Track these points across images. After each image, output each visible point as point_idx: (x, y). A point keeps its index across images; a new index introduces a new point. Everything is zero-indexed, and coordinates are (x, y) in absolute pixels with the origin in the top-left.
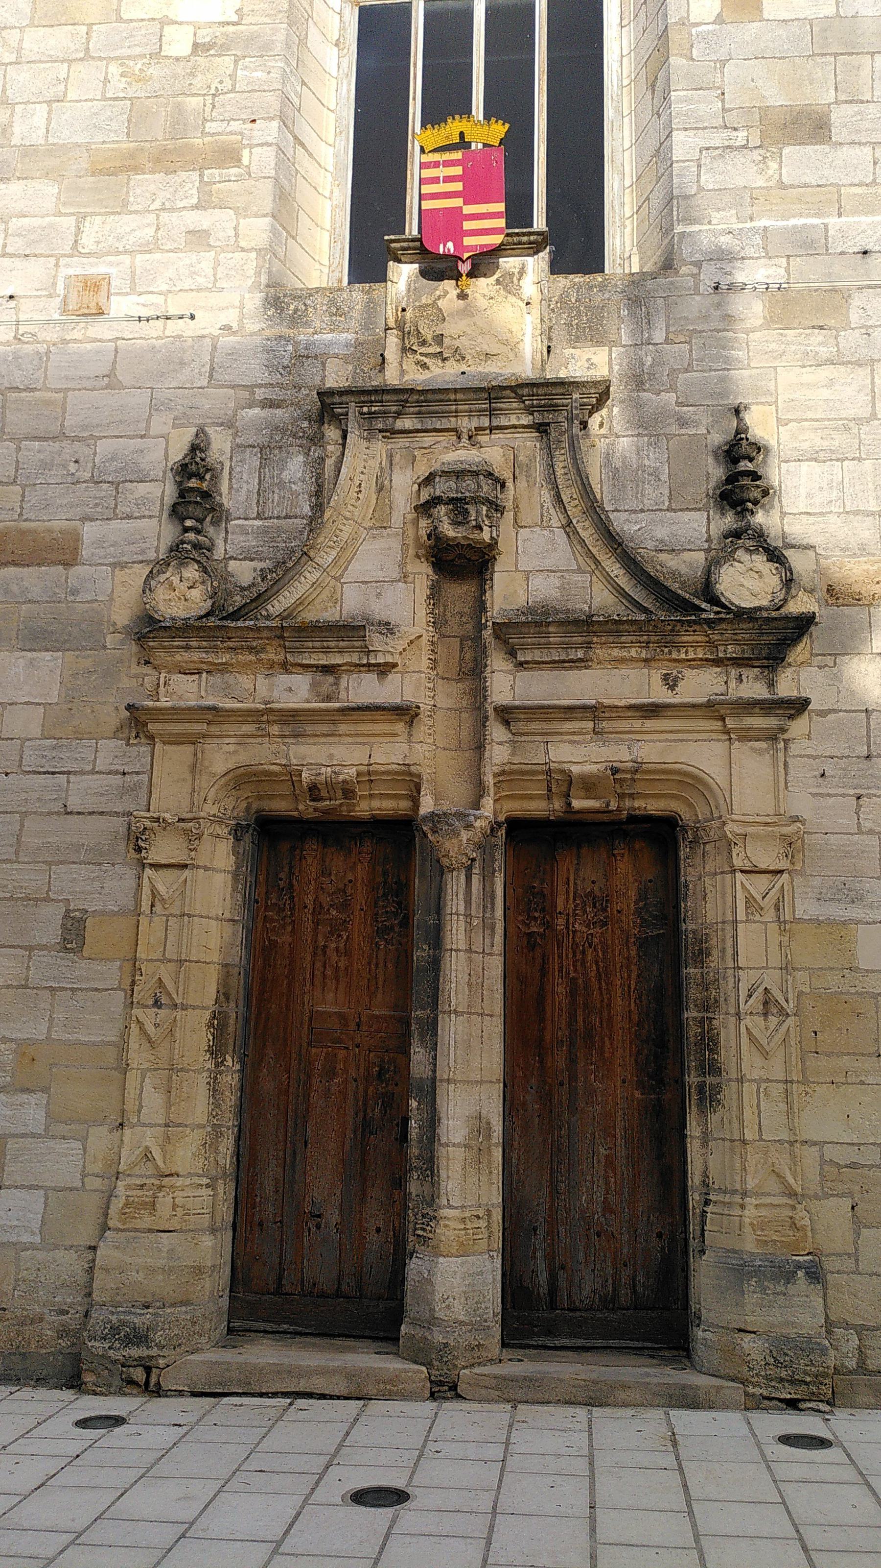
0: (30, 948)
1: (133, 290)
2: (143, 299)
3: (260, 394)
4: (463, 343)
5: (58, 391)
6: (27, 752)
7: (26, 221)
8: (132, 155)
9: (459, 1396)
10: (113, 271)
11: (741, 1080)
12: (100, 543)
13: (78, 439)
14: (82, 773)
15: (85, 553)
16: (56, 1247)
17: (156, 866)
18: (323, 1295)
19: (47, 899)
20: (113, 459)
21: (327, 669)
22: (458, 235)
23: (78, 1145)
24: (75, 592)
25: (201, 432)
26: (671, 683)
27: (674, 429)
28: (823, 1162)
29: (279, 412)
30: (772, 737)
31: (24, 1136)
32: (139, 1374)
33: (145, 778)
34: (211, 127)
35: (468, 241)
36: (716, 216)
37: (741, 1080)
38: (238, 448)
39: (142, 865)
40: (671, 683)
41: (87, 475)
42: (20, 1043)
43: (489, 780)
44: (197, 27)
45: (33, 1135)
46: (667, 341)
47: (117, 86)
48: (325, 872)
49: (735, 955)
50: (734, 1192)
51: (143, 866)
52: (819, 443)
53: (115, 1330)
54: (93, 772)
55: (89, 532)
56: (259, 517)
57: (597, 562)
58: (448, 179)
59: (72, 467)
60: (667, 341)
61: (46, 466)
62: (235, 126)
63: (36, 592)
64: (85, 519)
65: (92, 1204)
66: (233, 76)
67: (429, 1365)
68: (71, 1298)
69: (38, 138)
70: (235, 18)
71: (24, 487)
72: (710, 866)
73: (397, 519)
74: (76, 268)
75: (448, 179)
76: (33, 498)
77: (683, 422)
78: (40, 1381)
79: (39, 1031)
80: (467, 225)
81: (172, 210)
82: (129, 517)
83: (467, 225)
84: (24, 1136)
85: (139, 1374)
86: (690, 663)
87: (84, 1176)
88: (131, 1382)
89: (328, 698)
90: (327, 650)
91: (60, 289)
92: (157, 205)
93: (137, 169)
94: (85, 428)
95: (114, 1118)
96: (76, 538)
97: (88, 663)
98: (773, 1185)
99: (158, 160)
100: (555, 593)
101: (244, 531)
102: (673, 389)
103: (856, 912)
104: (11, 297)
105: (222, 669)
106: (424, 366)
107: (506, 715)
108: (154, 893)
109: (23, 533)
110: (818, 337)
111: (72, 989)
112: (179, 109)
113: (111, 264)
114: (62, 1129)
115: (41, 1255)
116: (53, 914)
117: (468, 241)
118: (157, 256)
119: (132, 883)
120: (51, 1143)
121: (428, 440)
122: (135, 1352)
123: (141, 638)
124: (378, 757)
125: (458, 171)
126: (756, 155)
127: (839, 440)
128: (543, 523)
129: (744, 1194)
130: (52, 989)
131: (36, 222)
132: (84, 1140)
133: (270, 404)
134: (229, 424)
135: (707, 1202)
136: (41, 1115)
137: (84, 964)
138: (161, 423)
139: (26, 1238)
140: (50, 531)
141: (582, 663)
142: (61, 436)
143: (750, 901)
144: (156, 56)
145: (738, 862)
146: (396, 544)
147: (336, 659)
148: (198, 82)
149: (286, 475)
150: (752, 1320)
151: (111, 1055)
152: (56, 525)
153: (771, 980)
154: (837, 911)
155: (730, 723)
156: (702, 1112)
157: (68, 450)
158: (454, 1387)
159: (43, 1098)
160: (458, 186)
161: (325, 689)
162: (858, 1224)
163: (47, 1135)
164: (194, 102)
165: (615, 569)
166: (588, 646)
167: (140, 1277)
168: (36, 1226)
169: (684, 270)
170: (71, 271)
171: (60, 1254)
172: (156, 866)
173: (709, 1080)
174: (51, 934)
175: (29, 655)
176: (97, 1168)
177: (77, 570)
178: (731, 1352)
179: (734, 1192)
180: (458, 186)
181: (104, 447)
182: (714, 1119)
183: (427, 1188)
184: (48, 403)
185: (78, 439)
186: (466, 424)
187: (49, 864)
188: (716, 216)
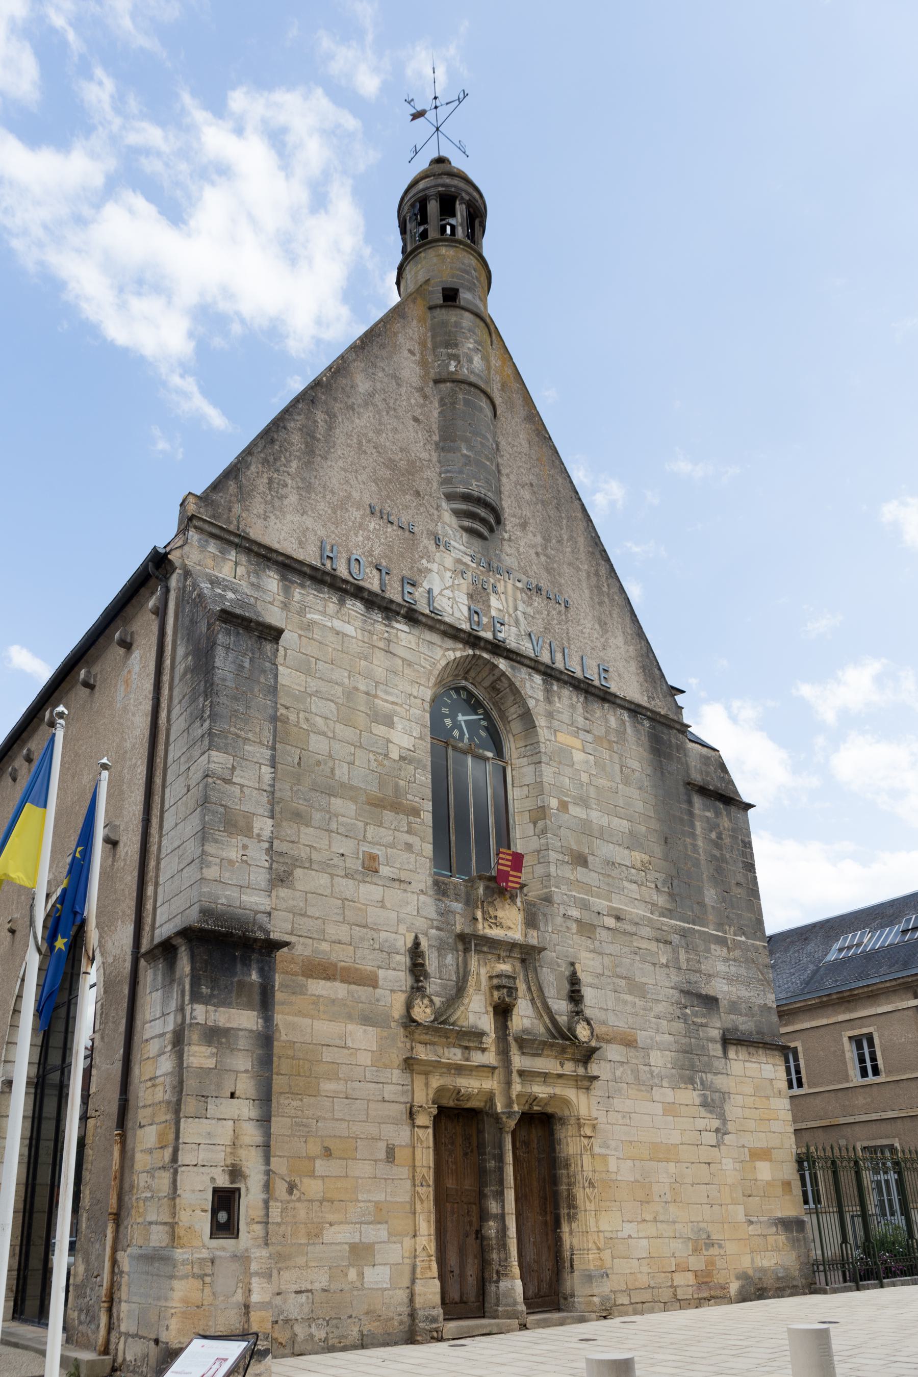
0: (376, 1161)
1: (387, 865)
2: (391, 869)
3: (435, 923)
4: (503, 921)
5: (364, 904)
6: (367, 1072)
7: (345, 819)
8: (382, 800)
9: (527, 1329)
10: (379, 853)
11: (586, 1211)
12: (385, 979)
13: (374, 929)
14: (388, 1083)
15: (380, 983)
16: (396, 1288)
17: (419, 1127)
18: (456, 1303)
19: (380, 1139)
20: (386, 941)
21: (467, 1048)
22: (507, 881)
23: (399, 1245)
24: (378, 1000)
25: (416, 937)
26: (562, 1065)
27: (556, 967)
28: (605, 1238)
29: (442, 933)
30: (588, 1089)
31: (381, 1242)
32: (435, 1334)
33: (409, 1087)
34: (409, 797)
35: (510, 884)
36: (562, 887)
37: (586, 1211)
38: (429, 946)
39: (413, 1125)
40: (562, 1065)
41: (377, 947)
42: (376, 1203)
43: (514, 1097)
44: (400, 748)
45: (384, 1242)
46: (553, 932)
47: (374, 765)
48: (446, 1129)
49: (582, 1166)
50: (584, 1250)
51: (414, 1127)
52: (593, 982)
53: (427, 1318)
54: (391, 1083)
55: (381, 973)
56: (440, 978)
57: (542, 1016)
58: (507, 860)
59: (371, 942)
60: (553, 932)
61: (362, 939)
62: (417, 799)
63: (363, 999)
64: (379, 967)
65: (407, 1270)
66: (414, 775)
67: (518, 1318)
68: (405, 1310)
69: (345, 779)
70: (412, 749)
71: (355, 947)
72: (570, 1133)
73: (483, 988)
74: (365, 848)
75: (507, 860)
76: (359, 953)
77: (559, 966)
78: (396, 1344)
79: (380, 1197)
80: (511, 878)
81: (399, 831)
82: (394, 969)
83: (511, 878)
84: (381, 1242)
85: (435, 1334)
86: (568, 1059)
87: (403, 1258)
88: (432, 1338)
89: (467, 1060)
90: (469, 1040)
91: (361, 856)
92: (392, 827)
93: (384, 808)
94: (375, 924)
95: (412, 1233)
96: (377, 976)
97: (385, 1034)
98: (594, 1247)
99: (392, 806)
100: (530, 1026)
101: (435, 983)
102: (555, 951)
103: (608, 1152)
104: (343, 855)
105: (433, 1044)
106: (491, 927)
107: (521, 1073)
108: (419, 1138)
109: (357, 969)
110: (589, 941)
111: (393, 1179)
112: (397, 784)
113: (378, 850)
114: (393, 1239)
115: (391, 1292)
116: (382, 1145)
117: (510, 884)
118: (395, 851)
119: (408, 1133)
120: (390, 1245)
121: (490, 957)
122: (434, 1326)
123: (405, 1026)
124: (484, 1086)
125: (510, 858)
126: (571, 866)
127: (596, 981)
128: (524, 998)
129: (588, 1250)
130: (385, 1179)
131: (349, 820)
132: (402, 1243)
133: (438, 929)
134: (426, 934)
135: (572, 1255)
136: (386, 1233)
137: (395, 1168)
138: (402, 929)
139: (385, 1286)
140: (366, 970)
141: (539, 1055)
142: (365, 926)
143: (585, 1146)
144: (386, 755)
145: (582, 1133)
146: (483, 998)
147: (471, 1045)
148: (402, 773)
149: (447, 962)
150: (596, 1291)
151: (408, 1207)
152: (369, 968)
153: (590, 1175)
154: (603, 1151)
155: (579, 1083)
156: (570, 1222)
157: (371, 934)
158: (525, 1325)
159: (384, 1226)
160: (509, 863)
161: (466, 1055)
162: (613, 1258)
163: (388, 1242)
164: (402, 783)
165: (547, 1021)
166: (543, 1049)
167: (431, 1297)
168: (388, 1280)
169: (556, 905)
170: (364, 849)
171: (397, 1291)
172: (419, 1127)
173: (572, 1211)
174: (382, 1155)
175: (364, 1027)
176: (406, 1255)
177: (378, 991)
178: (590, 1303)
179: (584, 1250)
180: (509, 863)
181: (383, 935)
182: (574, 1225)
183: (502, 1256)
184: (360, 909)
185: (374, 929)
186: (503, 954)
187: (379, 1123)
188: (562, 887)
